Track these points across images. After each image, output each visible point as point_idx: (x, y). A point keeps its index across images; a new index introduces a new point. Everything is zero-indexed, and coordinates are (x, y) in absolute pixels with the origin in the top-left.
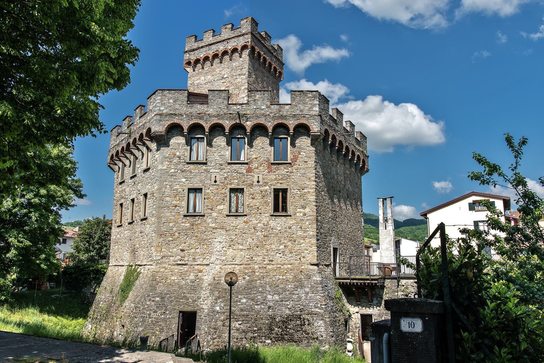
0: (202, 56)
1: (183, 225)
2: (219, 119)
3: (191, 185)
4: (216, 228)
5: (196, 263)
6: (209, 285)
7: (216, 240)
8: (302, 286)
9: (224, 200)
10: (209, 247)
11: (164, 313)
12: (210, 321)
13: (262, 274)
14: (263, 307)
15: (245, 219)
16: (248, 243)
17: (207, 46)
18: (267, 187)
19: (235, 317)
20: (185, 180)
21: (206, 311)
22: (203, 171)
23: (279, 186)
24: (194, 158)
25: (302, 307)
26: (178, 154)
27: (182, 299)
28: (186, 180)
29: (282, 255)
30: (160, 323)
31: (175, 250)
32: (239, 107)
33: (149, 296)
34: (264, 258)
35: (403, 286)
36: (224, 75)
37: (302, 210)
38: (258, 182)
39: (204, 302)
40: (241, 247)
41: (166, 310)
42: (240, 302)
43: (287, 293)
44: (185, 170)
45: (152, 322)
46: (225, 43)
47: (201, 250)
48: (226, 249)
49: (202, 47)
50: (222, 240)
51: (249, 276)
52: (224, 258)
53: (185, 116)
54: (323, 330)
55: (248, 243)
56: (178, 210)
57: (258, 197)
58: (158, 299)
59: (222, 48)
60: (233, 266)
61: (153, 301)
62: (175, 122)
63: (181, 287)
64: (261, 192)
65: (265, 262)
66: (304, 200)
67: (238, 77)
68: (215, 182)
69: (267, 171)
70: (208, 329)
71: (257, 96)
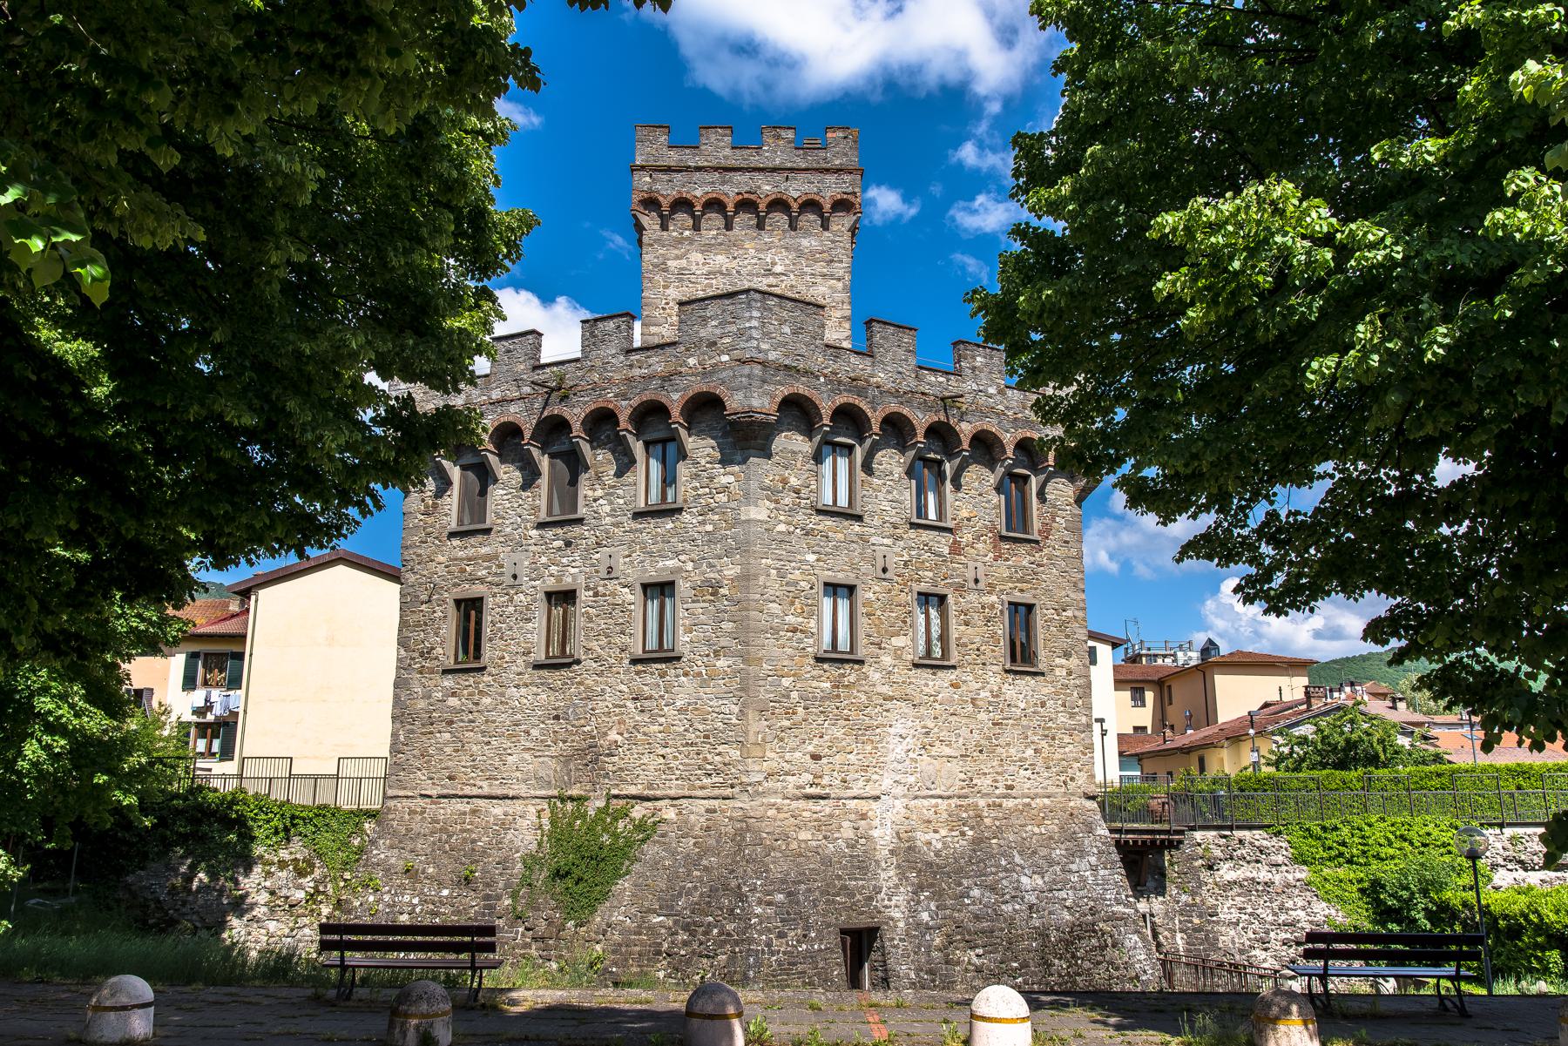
0: (698, 193)
1: (815, 684)
2: (902, 403)
3: (830, 573)
4: (891, 698)
5: (850, 793)
6: (892, 852)
7: (892, 731)
8: (1083, 854)
9: (905, 622)
10: (876, 748)
11: (805, 936)
12: (915, 953)
13: (997, 823)
14: (1017, 907)
15: (953, 677)
16: (961, 740)
17: (716, 169)
18: (994, 598)
19: (967, 937)
21: (901, 924)
22: (855, 539)
23: (1018, 597)
25: (1092, 903)
26: (794, 481)
27: (838, 895)
28: (818, 560)
29: (1029, 772)
30: (800, 968)
31: (798, 755)
32: (941, 379)
33: (755, 889)
34: (996, 781)
35: (1199, 845)
36: (774, 264)
37: (1063, 661)
38: (976, 581)
39: (890, 900)
40: (947, 751)
41: (807, 928)
42: (968, 897)
43: (1058, 868)
44: (813, 530)
45: (779, 965)
46: (778, 177)
47: (860, 757)
48: (915, 756)
49: (699, 169)
50: (903, 732)
51: (972, 828)
52: (911, 779)
53: (822, 379)
54: (1143, 957)
55: (961, 740)
56: (800, 641)
57: (977, 619)
58: (780, 897)
59: (768, 188)
60: (934, 801)
61: (769, 904)
62: (801, 392)
63: (827, 862)
64: (983, 607)
65: (997, 792)
66: (1067, 636)
67: (819, 280)
68: (885, 570)
69: (991, 555)
70: (917, 975)
71: (979, 359)
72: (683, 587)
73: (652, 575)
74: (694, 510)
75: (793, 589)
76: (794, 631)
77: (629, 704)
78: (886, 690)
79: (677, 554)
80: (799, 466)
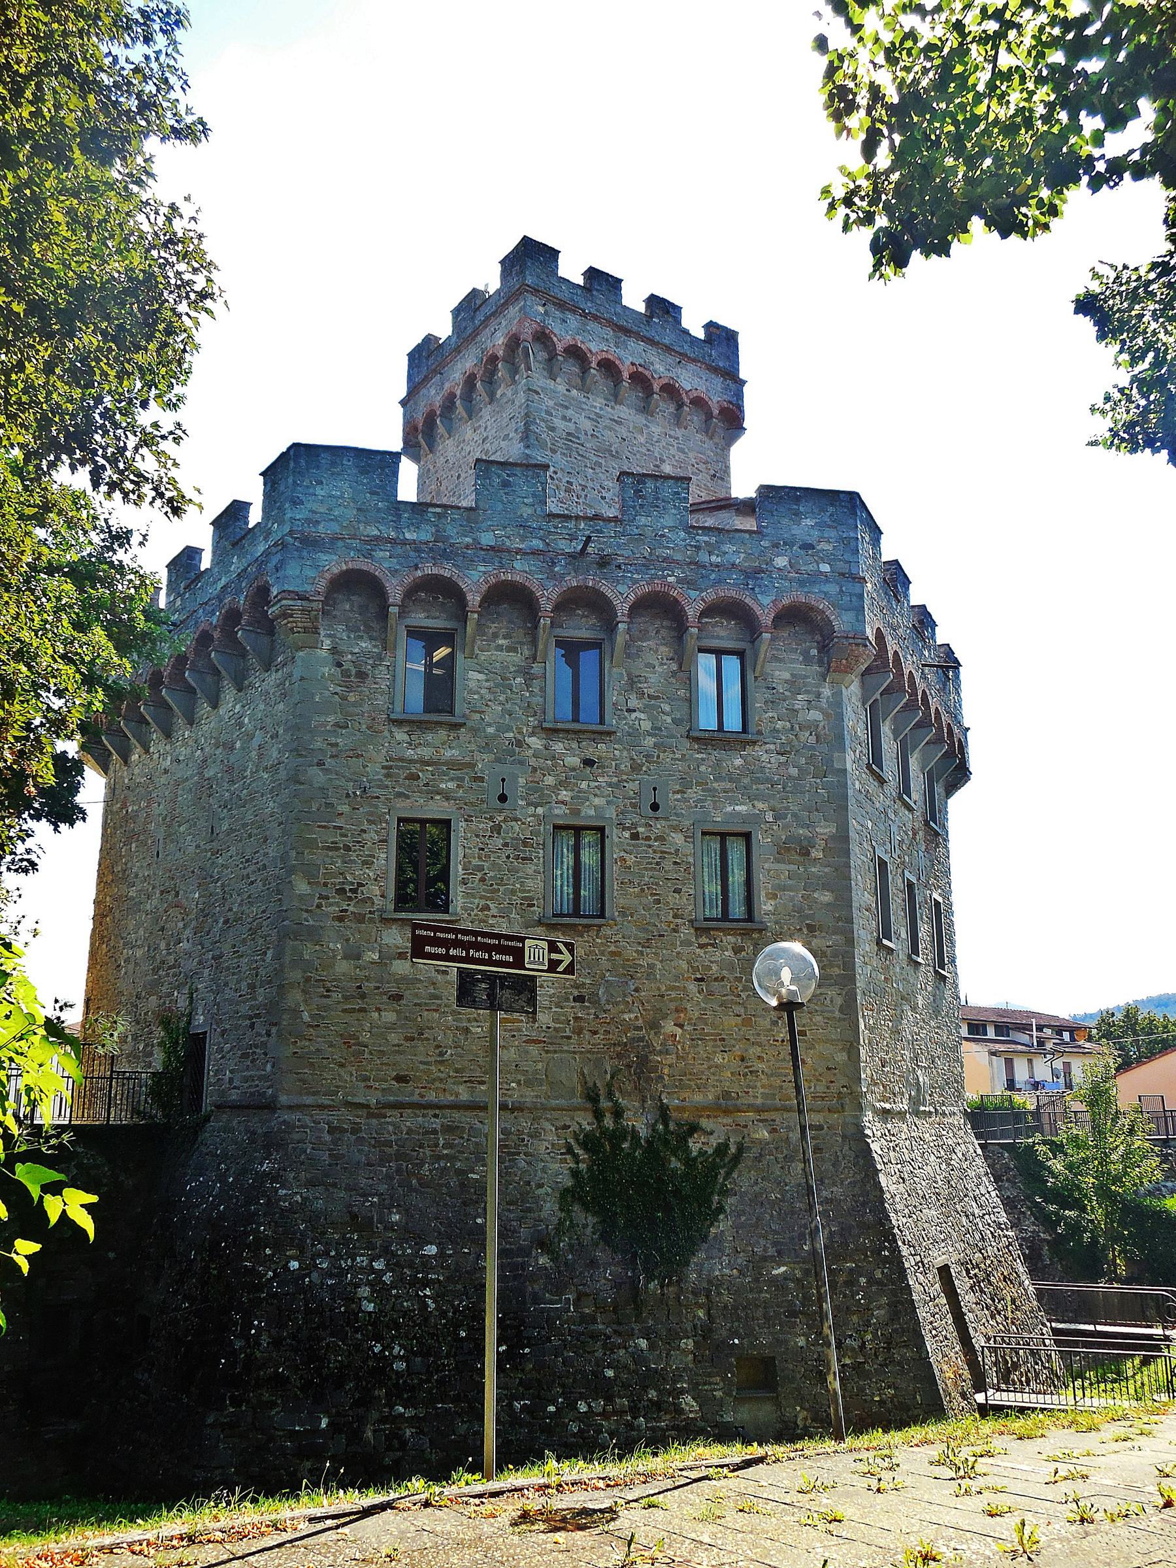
77: (692, 987)
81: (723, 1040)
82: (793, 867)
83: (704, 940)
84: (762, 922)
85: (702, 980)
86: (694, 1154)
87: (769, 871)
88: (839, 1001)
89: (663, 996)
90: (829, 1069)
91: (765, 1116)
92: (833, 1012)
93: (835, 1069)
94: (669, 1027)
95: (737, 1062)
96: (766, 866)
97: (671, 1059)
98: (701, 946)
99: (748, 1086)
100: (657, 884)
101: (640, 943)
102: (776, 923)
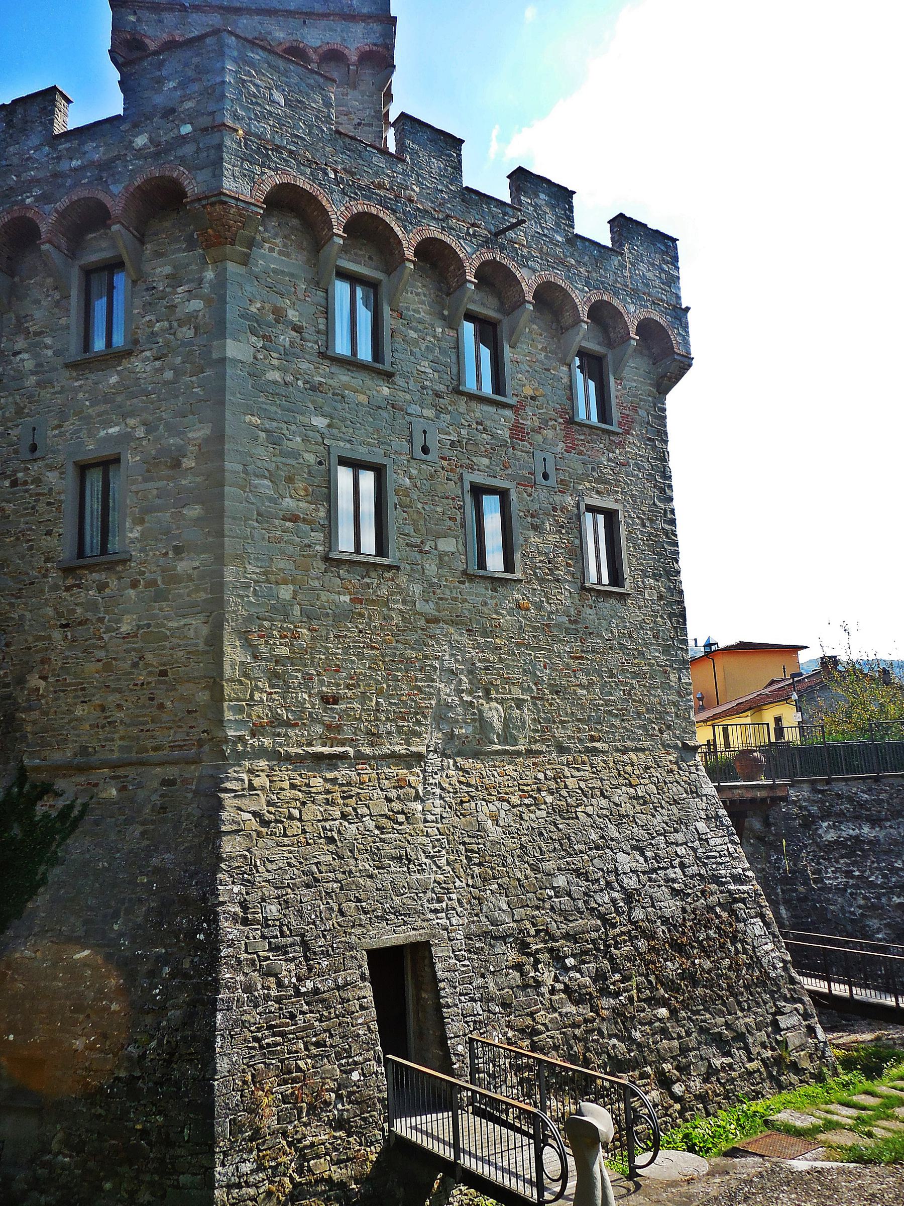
4: (436, 621)
20: (326, 421)
24: (342, 347)
28: (329, 426)
38: (546, 476)
44: (320, 384)
72: (131, 459)
73: (91, 449)
74: (148, 354)
75: (292, 462)
76: (294, 519)
77: (57, 635)
78: (429, 608)
79: (124, 416)
80: (301, 296)
81: (83, 689)
82: (162, 483)
83: (70, 582)
84: (125, 552)
85: (66, 626)
86: (37, 819)
87: (137, 493)
88: (205, 630)
89: (29, 648)
90: (189, 712)
91: (121, 772)
92: (196, 645)
93: (196, 711)
94: (34, 681)
95: (98, 713)
96: (134, 488)
97: (35, 715)
98: (68, 589)
99: (106, 740)
100: (31, 529)
101: (13, 595)
102: (141, 551)
